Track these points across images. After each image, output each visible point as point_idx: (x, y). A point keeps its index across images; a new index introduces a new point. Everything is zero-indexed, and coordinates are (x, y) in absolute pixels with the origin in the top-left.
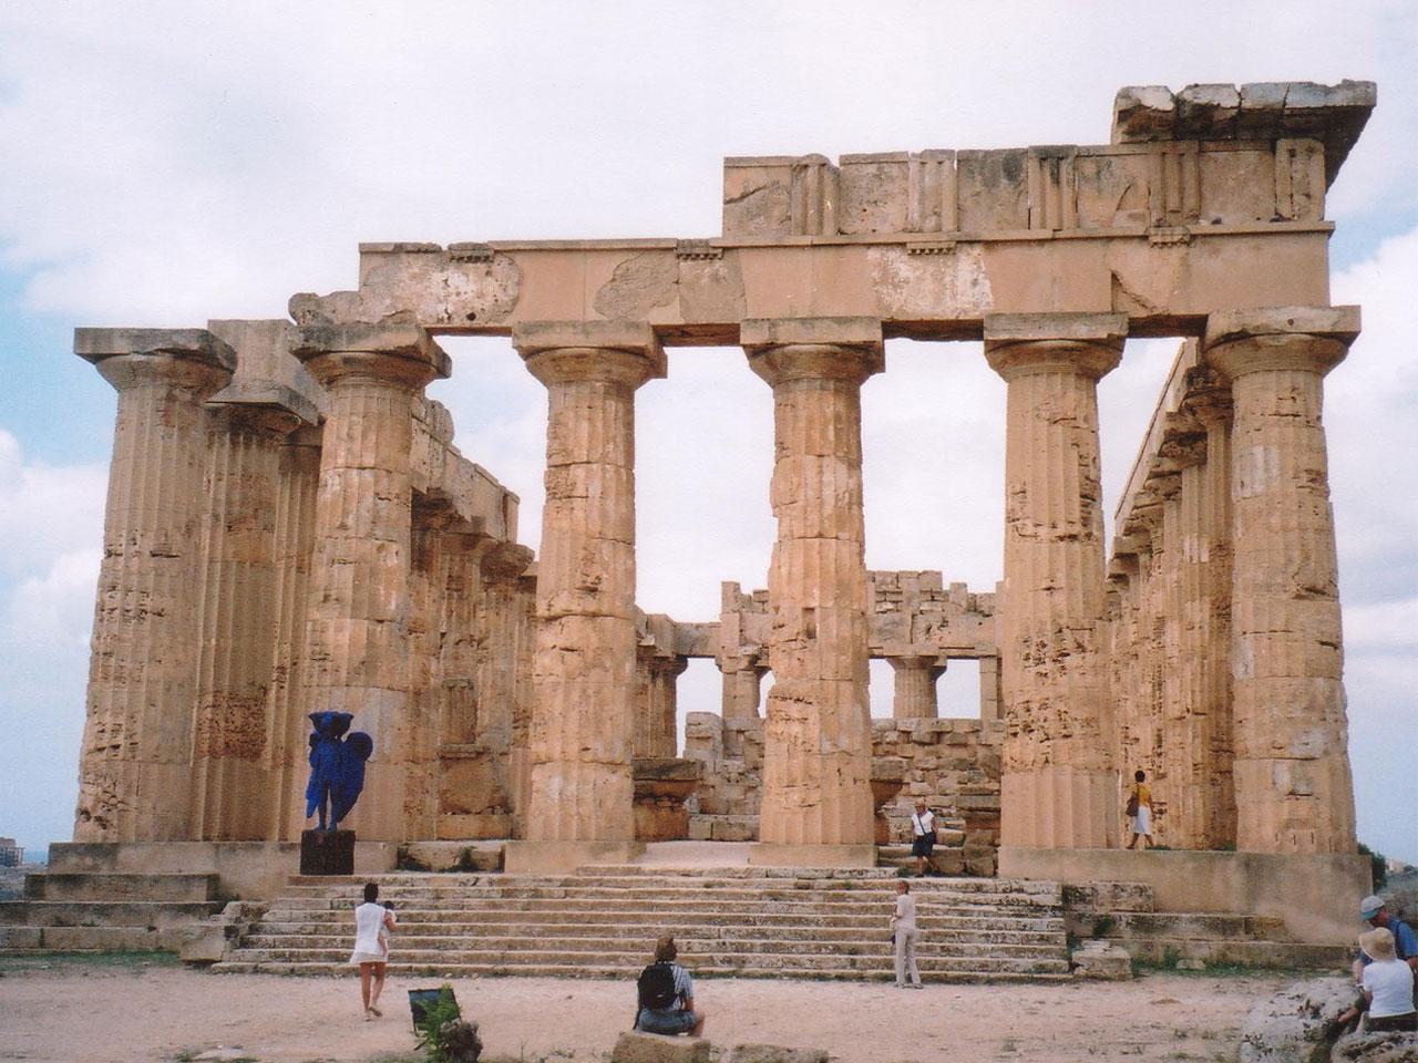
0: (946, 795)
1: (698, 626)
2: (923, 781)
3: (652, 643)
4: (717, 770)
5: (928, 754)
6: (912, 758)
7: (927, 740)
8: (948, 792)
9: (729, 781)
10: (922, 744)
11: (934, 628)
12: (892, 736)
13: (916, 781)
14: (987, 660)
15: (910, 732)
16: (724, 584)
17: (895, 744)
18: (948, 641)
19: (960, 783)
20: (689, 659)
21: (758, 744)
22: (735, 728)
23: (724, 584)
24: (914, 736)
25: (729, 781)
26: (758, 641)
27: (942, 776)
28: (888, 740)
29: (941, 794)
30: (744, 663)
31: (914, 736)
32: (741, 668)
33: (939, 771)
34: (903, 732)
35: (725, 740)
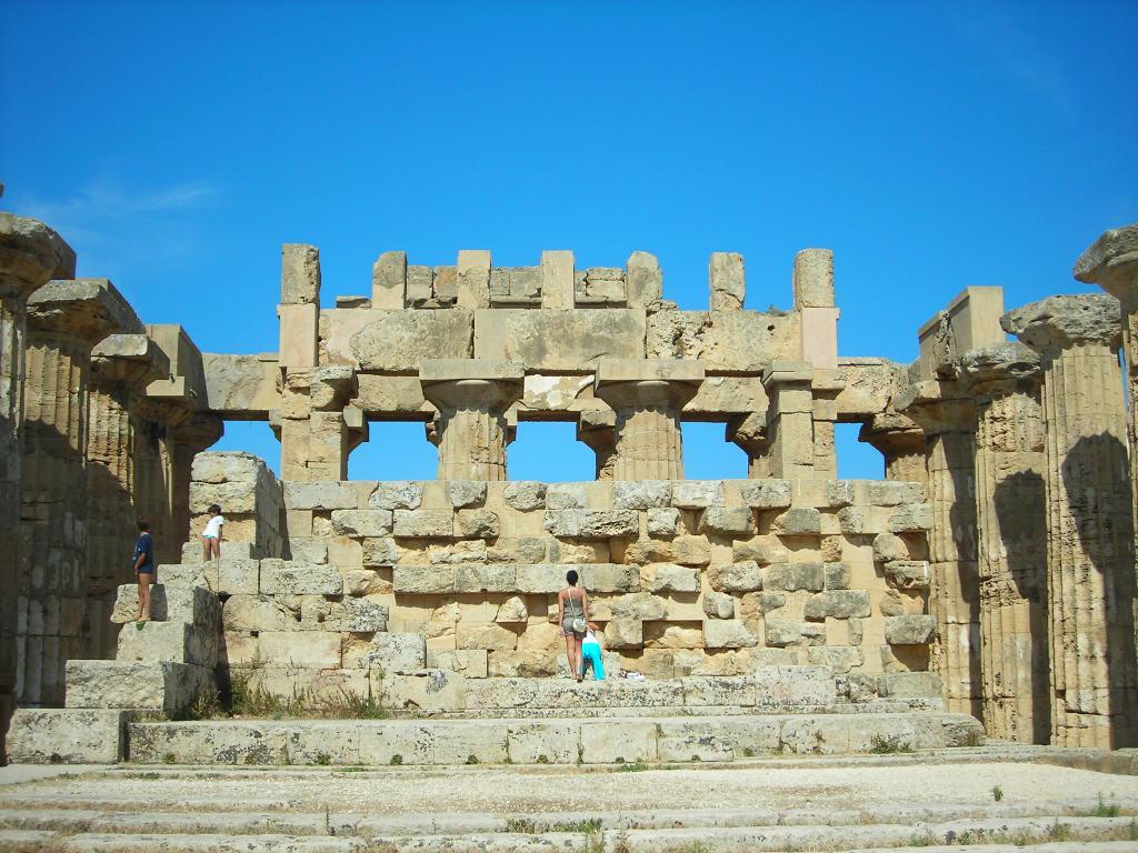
0: (782, 645)
2: (732, 617)
5: (740, 557)
6: (704, 566)
7: (739, 524)
8: (785, 639)
9: (299, 618)
11: (688, 335)
12: (665, 519)
15: (701, 510)
17: (669, 536)
18: (715, 360)
19: (809, 619)
20: (227, 424)
21: (361, 540)
24: (712, 519)
25: (299, 618)
26: (352, 358)
27: (775, 605)
28: (654, 527)
29: (769, 645)
30: (326, 395)
32: (318, 405)
34: (684, 509)
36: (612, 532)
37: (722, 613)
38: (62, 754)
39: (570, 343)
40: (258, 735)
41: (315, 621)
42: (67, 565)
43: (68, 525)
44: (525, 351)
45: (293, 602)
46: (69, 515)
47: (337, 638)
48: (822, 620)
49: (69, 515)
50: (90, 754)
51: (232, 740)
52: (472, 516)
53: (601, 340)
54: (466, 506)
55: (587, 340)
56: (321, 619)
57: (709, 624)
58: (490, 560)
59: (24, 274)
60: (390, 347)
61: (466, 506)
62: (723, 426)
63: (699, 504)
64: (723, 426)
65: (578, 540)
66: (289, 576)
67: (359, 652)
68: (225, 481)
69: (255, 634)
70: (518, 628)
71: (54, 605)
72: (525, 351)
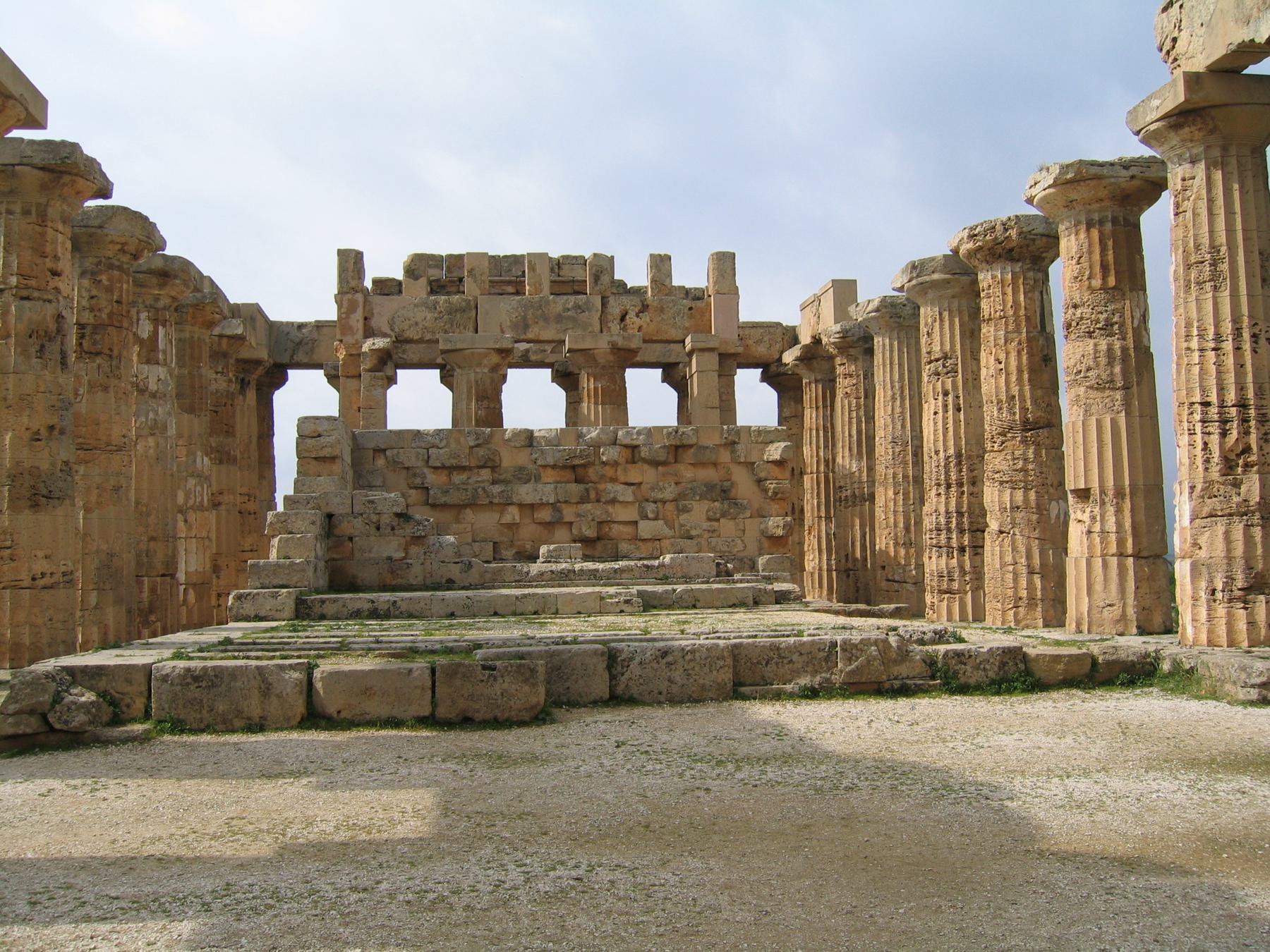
0: (691, 538)
1: (301, 326)
2: (656, 519)
3: (240, 331)
4: (357, 509)
7: (662, 456)
8: (693, 533)
9: (378, 528)
10: (655, 463)
11: (631, 314)
13: (647, 518)
14: (706, 354)
15: (636, 447)
16: (341, 253)
17: (615, 464)
19: (710, 519)
21: (408, 468)
22: (372, 445)
23: (341, 253)
25: (378, 528)
26: (389, 332)
27: (686, 510)
31: (644, 452)
33: (682, 503)
34: (626, 446)
35: (356, 464)
36: (576, 462)
37: (650, 515)
38: (262, 614)
39: (546, 320)
40: (373, 602)
41: (389, 529)
42: (199, 488)
43: (199, 460)
44: (515, 327)
45: (374, 518)
46: (199, 453)
47: (403, 541)
48: (718, 520)
49: (199, 453)
50: (278, 615)
51: (358, 605)
52: (481, 452)
53: (569, 318)
54: (477, 446)
55: (559, 318)
56: (393, 529)
57: (643, 525)
58: (494, 482)
59: (173, 293)
60: (417, 324)
61: (477, 446)
62: (659, 371)
63: (635, 443)
64: (659, 371)
65: (554, 467)
66: (372, 502)
67: (414, 550)
68: (319, 436)
69: (351, 539)
70: (512, 526)
71: (192, 516)
72: (515, 327)
